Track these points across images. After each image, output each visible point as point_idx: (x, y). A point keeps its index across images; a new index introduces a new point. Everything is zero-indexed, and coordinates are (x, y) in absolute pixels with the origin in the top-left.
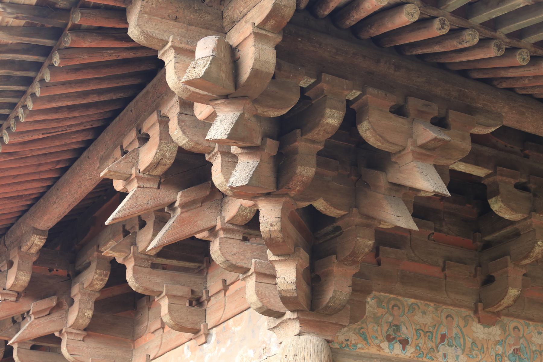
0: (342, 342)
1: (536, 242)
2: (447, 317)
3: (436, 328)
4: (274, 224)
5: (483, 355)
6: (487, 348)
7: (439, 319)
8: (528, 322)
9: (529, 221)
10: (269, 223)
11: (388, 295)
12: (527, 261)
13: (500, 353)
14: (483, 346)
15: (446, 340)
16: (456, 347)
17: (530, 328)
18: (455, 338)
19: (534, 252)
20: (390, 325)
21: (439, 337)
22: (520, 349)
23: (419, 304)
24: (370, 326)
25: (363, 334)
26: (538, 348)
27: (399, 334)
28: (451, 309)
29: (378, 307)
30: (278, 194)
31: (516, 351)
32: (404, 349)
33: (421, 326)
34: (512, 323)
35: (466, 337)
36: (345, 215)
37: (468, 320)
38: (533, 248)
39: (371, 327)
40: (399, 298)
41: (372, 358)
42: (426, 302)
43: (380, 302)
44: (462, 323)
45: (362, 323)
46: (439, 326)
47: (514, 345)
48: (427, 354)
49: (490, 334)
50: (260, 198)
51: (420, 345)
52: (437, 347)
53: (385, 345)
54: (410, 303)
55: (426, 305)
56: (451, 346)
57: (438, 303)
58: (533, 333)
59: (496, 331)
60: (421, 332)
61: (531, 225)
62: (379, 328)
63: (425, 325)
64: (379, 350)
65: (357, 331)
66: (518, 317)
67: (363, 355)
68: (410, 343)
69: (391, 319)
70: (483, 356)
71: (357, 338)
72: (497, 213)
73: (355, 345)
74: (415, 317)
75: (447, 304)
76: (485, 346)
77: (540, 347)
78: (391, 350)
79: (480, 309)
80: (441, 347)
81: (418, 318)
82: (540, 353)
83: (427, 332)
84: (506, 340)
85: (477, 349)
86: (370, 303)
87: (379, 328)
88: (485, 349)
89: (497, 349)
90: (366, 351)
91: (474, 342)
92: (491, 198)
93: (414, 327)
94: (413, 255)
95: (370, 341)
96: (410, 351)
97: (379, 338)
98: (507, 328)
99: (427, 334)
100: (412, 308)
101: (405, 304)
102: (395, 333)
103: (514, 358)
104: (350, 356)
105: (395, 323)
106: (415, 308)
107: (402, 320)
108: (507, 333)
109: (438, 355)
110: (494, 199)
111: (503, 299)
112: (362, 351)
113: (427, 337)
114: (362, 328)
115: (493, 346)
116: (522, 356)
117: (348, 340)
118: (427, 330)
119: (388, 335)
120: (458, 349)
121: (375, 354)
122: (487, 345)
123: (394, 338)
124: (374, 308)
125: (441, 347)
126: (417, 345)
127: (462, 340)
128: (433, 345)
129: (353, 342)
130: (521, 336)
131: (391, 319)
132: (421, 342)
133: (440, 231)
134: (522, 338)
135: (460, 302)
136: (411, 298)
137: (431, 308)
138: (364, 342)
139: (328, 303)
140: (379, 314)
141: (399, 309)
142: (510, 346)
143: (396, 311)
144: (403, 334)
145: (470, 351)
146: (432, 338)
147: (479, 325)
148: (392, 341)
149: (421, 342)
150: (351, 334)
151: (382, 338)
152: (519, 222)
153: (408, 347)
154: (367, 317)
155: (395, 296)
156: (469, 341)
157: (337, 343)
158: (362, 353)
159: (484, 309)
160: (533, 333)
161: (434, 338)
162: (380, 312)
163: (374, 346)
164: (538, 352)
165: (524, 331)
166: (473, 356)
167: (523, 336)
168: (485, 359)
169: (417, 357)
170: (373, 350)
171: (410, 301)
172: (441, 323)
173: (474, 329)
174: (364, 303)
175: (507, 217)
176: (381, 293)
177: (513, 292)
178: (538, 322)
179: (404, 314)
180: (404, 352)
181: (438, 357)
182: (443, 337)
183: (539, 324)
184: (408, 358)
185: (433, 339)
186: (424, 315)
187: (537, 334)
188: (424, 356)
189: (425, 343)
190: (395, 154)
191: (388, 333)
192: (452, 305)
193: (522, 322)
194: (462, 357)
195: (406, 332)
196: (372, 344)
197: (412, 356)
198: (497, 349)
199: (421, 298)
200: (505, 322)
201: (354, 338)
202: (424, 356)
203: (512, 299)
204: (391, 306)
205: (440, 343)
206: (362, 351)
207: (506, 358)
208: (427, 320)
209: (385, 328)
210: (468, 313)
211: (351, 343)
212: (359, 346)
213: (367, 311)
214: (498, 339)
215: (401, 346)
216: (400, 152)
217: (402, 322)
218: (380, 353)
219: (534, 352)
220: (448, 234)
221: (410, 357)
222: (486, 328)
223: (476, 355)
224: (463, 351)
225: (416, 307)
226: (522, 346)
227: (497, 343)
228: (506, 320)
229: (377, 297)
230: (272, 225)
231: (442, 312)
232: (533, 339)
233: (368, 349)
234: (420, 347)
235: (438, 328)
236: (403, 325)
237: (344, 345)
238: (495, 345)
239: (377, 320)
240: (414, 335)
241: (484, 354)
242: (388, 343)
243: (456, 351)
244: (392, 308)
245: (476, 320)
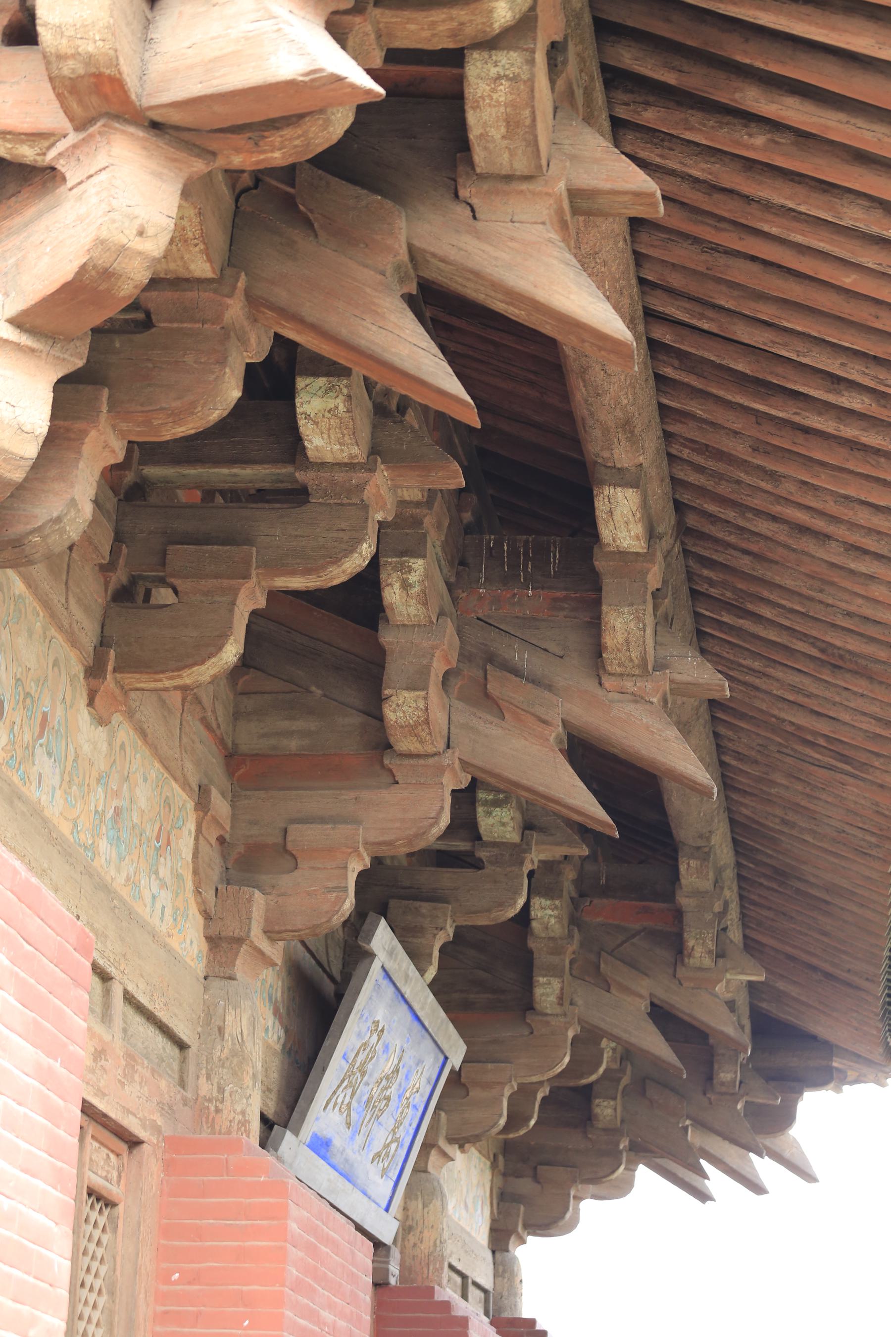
1: (360, 541)
4: (150, 231)
9: (357, 477)
10: (138, 222)
30: (187, 142)
36: (200, 282)
50: (131, 129)
61: (361, 488)
92: (316, 374)
110: (322, 381)
139: (32, 532)
152: (322, 465)
190: (482, 177)
216: (508, 178)
230: (141, 233)
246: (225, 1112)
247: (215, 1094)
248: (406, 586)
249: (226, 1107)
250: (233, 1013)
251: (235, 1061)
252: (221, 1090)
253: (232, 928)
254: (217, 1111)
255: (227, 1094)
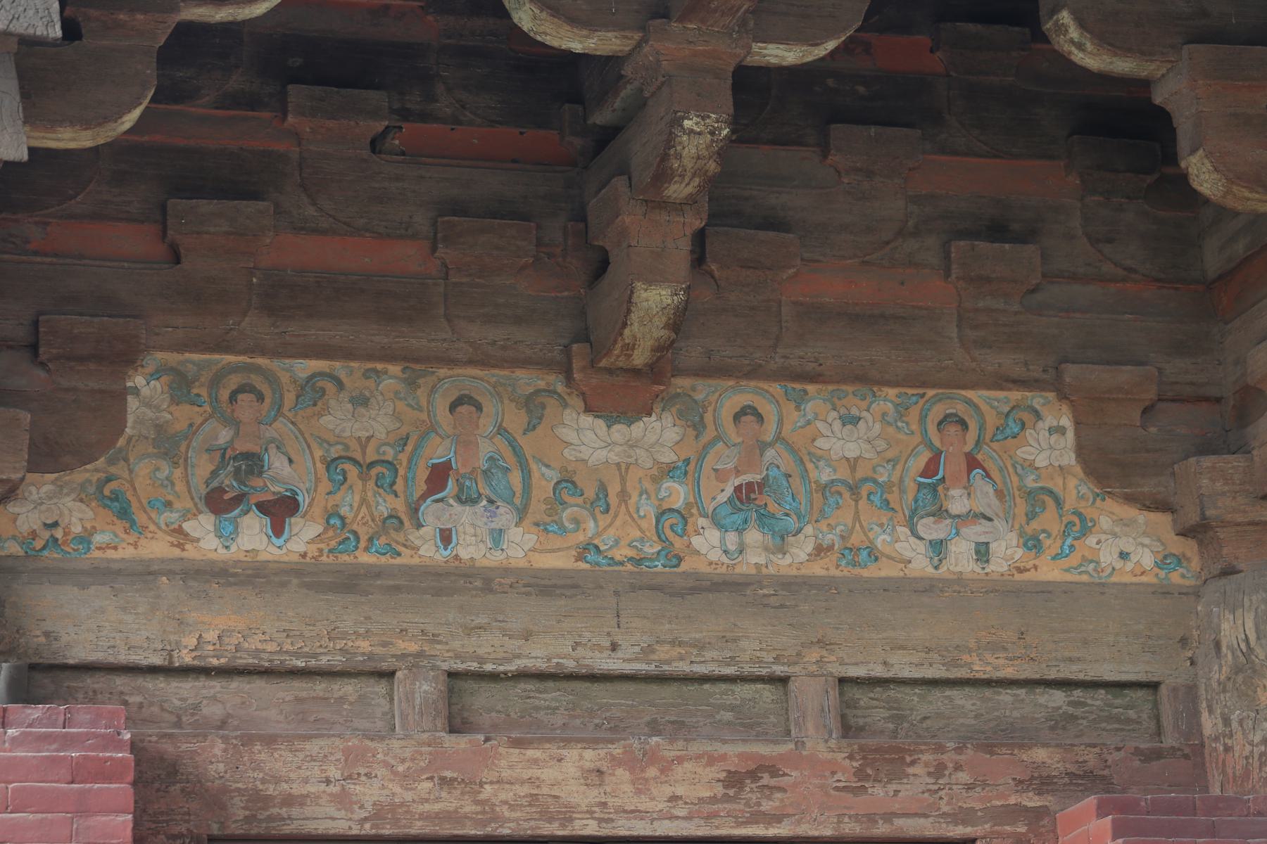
0: (34, 534)
1: (677, 122)
2: (453, 407)
3: (409, 448)
5: (603, 520)
6: (624, 495)
7: (424, 416)
8: (798, 386)
11: (217, 357)
12: (677, 190)
13: (679, 504)
14: (603, 488)
15: (451, 483)
16: (491, 502)
17: (809, 407)
18: (485, 472)
19: (679, 156)
20: (224, 456)
21: (423, 474)
22: (762, 485)
23: (342, 375)
24: (143, 469)
25: (117, 499)
26: (843, 473)
27: (258, 482)
28: (471, 379)
29: (175, 401)
31: (745, 495)
32: (278, 530)
33: (347, 447)
34: (727, 398)
35: (534, 466)
37: (543, 407)
38: (670, 141)
39: (145, 473)
40: (261, 361)
41: (150, 573)
42: (370, 365)
43: (181, 386)
44: (515, 419)
45: (111, 462)
46: (424, 436)
47: (738, 472)
48: (371, 540)
49: (632, 445)
51: (344, 511)
52: (414, 510)
53: (203, 527)
54: (304, 375)
55: (366, 375)
56: (467, 499)
57: (417, 360)
58: (820, 425)
59: (660, 433)
60: (348, 466)
62: (178, 473)
63: (364, 444)
64: (181, 546)
65: (92, 490)
66: (754, 373)
67: (115, 566)
68: (302, 509)
69: (224, 436)
70: (602, 524)
71: (90, 514)
72: (539, 38)
73: (85, 539)
74: (325, 420)
75: (451, 362)
76: (614, 489)
77: (853, 468)
78: (226, 539)
79: (577, 364)
80: (429, 510)
81: (339, 420)
82: (854, 489)
83: (372, 465)
84: (701, 458)
85: (580, 500)
86: (145, 391)
87: (178, 473)
88: (613, 500)
89: (663, 494)
90: (126, 552)
91: (567, 481)
93: (318, 453)
94: (311, 211)
95: (140, 518)
96: (303, 537)
97: (177, 505)
98: (708, 417)
99: (374, 472)
100: (312, 391)
101: (285, 378)
102: (241, 482)
103: (738, 518)
104: (60, 575)
105: (242, 446)
106: (323, 391)
107: (270, 433)
108: (710, 433)
109: (414, 536)
111: (625, 325)
112: (111, 554)
113: (371, 484)
114: (108, 480)
115: (647, 485)
116: (773, 507)
117: (56, 524)
118: (371, 456)
119: (213, 490)
120: (501, 510)
121: (163, 561)
122: (623, 480)
123: (239, 499)
124: (158, 408)
125: (429, 510)
126: (331, 514)
127: (516, 478)
128: (399, 505)
129: (77, 529)
130: (769, 437)
131: (224, 436)
132: (348, 502)
133: (424, 117)
134: (771, 445)
135: (504, 348)
136: (306, 356)
137: (387, 383)
138: (120, 526)
140: (181, 426)
141: (261, 398)
142: (720, 476)
143: (246, 408)
144: (274, 480)
145: (552, 511)
146: (393, 483)
147: (587, 420)
148: (228, 511)
149: (348, 502)
150: (69, 502)
151: (189, 505)
153: (295, 523)
154: (130, 438)
155: (241, 358)
156: (545, 479)
157: (14, 538)
158: (109, 561)
159: (593, 364)
160: (820, 425)
161: (399, 481)
162: (182, 416)
163: (160, 534)
164: (842, 489)
165: (780, 422)
166: (562, 527)
167: (779, 438)
168: (612, 531)
169: (330, 551)
170: (157, 548)
171: (306, 367)
172: (432, 428)
173: (568, 434)
174: (119, 397)
175: (577, 47)
176: (187, 355)
177: (655, 300)
178: (843, 380)
179: (279, 412)
180: (280, 542)
181: (418, 543)
182: (439, 476)
183: (849, 388)
184: (295, 558)
185: (399, 486)
186: (363, 410)
187: (837, 425)
188: (362, 544)
189: (364, 501)
191: (215, 484)
192: (471, 362)
193: (776, 388)
194: (515, 533)
195: (281, 473)
196: (152, 527)
197: (312, 550)
198: (663, 494)
199: (348, 354)
200: (699, 397)
201: (78, 517)
202: (362, 544)
203: (660, 321)
204: (225, 394)
205: (424, 497)
206: (111, 554)
207: (702, 522)
208: (377, 424)
209: (203, 467)
210: (542, 384)
211: (65, 534)
212: (98, 539)
213: (130, 420)
214: (668, 457)
215: (267, 521)
217: (273, 440)
218: (185, 554)
219: (824, 488)
220: (460, 123)
221: (304, 555)
222: (633, 427)
223: (576, 521)
224: (522, 513)
225: (330, 387)
226: (774, 472)
227: (668, 471)
228: (703, 389)
229: (172, 369)
231: (433, 390)
232: (820, 443)
233: (135, 545)
234: (342, 518)
235: (415, 449)
236: (273, 450)
237: (38, 544)
238: (656, 480)
239: (168, 445)
240: (318, 480)
241: (609, 518)
242: (212, 517)
243: (494, 515)
244: (233, 398)
245: (578, 403)
246: (1237, 748)
247: (1221, 727)
248: (1080, 47)
249: (1238, 742)
250: (1231, 617)
251: (1240, 678)
252: (1227, 721)
253: (1193, 518)
254: (1227, 749)
255: (1235, 725)
